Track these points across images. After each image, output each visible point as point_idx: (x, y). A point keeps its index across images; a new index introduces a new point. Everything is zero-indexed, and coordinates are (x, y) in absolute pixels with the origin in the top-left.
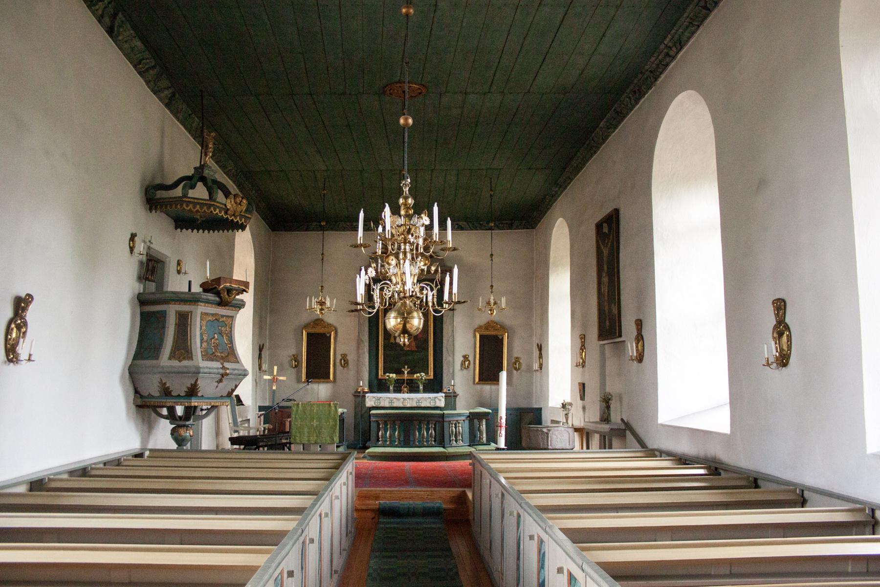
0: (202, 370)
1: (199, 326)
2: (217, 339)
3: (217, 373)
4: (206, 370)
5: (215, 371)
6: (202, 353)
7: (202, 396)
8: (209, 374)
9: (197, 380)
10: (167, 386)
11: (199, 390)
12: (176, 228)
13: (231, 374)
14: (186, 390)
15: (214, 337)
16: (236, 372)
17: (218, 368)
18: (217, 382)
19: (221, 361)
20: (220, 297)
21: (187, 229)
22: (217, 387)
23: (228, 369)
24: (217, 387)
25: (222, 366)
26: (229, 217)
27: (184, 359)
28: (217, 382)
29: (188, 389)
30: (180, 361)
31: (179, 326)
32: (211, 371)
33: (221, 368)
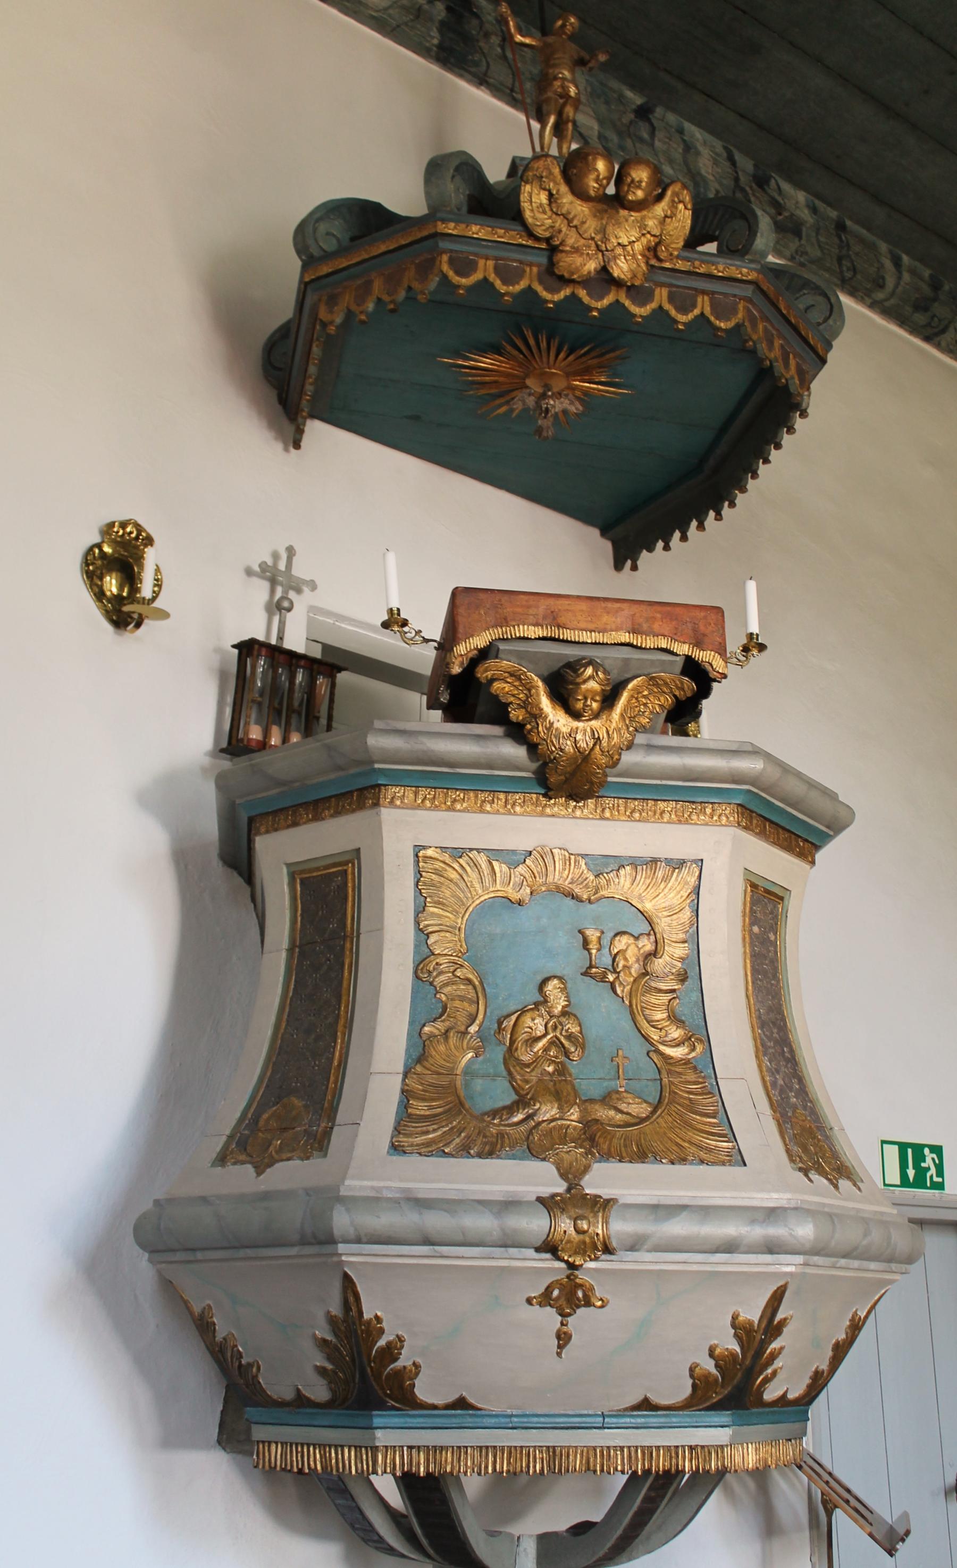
0: (341, 1221)
1: (409, 935)
2: (564, 1013)
3: (496, 1235)
4: (383, 1221)
5: (484, 1223)
6: (404, 1105)
7: (461, 1404)
8: (427, 1241)
9: (348, 1283)
10: (219, 1337)
11: (404, 1361)
12: (618, 566)
13: (634, 1245)
14: (320, 1360)
15: (543, 1002)
16: (678, 1228)
17: (509, 1205)
18: (546, 1299)
19: (572, 1153)
20: (517, 732)
21: (650, 549)
22: (563, 1338)
23: (601, 1205)
24: (563, 1338)
25: (560, 1187)
26: (582, 293)
27: (290, 1150)
28: (546, 1299)
29: (329, 1359)
30: (259, 1173)
31: (302, 955)
32: (435, 1221)
33: (549, 1204)
